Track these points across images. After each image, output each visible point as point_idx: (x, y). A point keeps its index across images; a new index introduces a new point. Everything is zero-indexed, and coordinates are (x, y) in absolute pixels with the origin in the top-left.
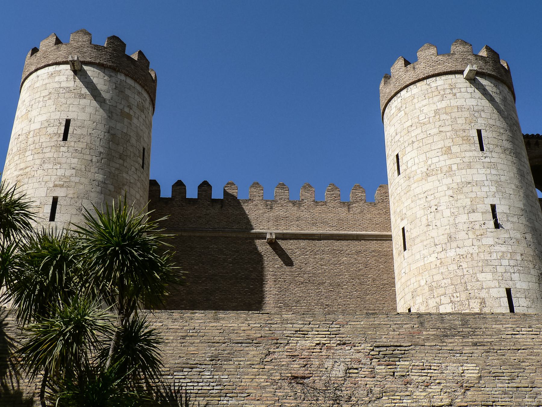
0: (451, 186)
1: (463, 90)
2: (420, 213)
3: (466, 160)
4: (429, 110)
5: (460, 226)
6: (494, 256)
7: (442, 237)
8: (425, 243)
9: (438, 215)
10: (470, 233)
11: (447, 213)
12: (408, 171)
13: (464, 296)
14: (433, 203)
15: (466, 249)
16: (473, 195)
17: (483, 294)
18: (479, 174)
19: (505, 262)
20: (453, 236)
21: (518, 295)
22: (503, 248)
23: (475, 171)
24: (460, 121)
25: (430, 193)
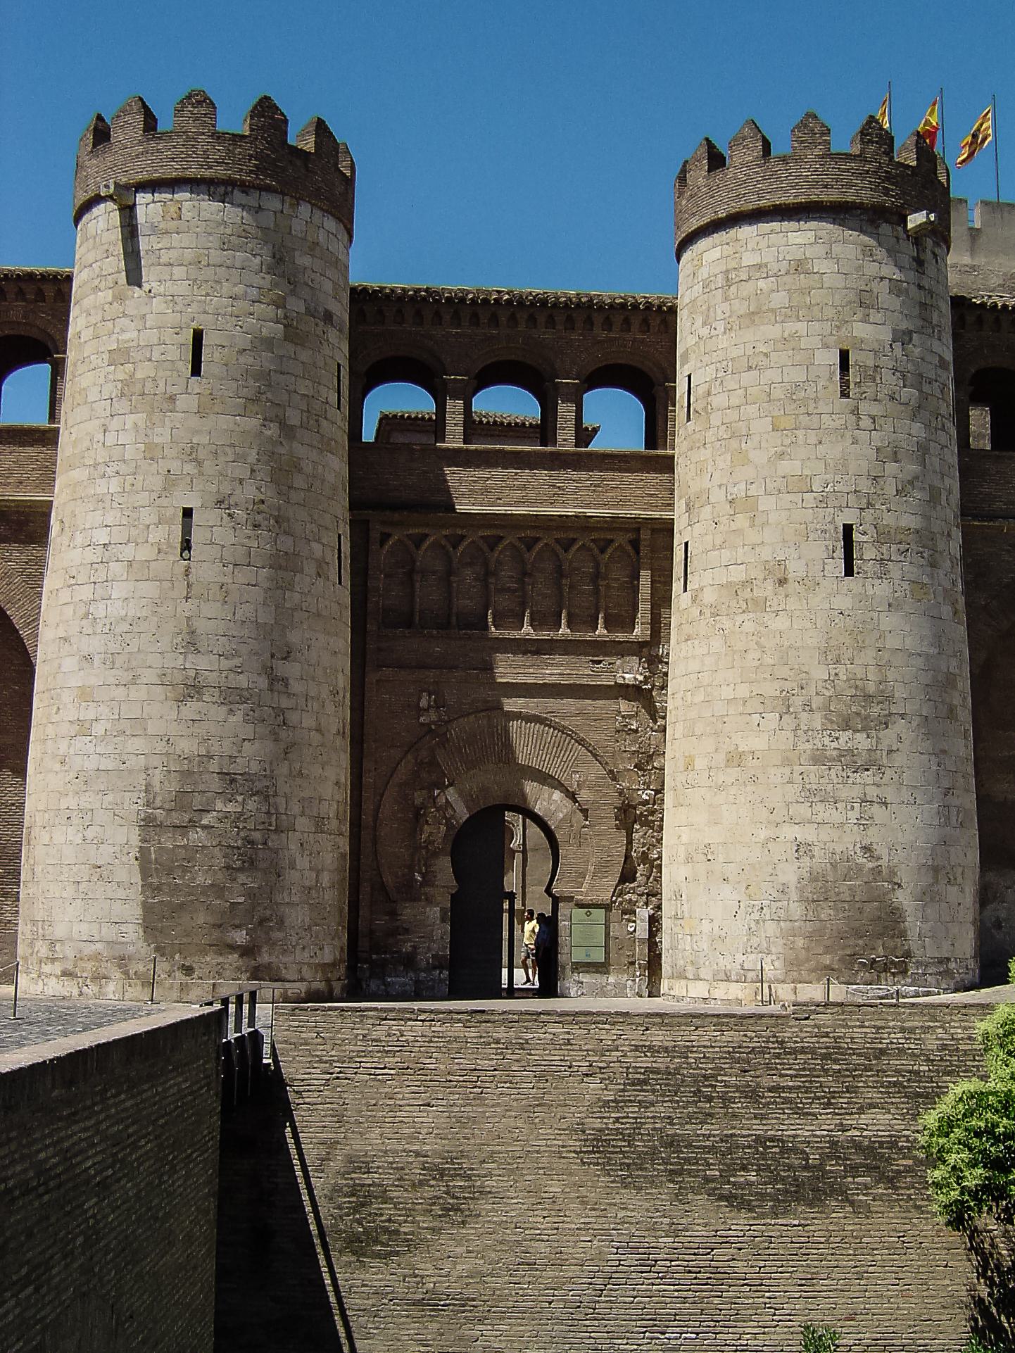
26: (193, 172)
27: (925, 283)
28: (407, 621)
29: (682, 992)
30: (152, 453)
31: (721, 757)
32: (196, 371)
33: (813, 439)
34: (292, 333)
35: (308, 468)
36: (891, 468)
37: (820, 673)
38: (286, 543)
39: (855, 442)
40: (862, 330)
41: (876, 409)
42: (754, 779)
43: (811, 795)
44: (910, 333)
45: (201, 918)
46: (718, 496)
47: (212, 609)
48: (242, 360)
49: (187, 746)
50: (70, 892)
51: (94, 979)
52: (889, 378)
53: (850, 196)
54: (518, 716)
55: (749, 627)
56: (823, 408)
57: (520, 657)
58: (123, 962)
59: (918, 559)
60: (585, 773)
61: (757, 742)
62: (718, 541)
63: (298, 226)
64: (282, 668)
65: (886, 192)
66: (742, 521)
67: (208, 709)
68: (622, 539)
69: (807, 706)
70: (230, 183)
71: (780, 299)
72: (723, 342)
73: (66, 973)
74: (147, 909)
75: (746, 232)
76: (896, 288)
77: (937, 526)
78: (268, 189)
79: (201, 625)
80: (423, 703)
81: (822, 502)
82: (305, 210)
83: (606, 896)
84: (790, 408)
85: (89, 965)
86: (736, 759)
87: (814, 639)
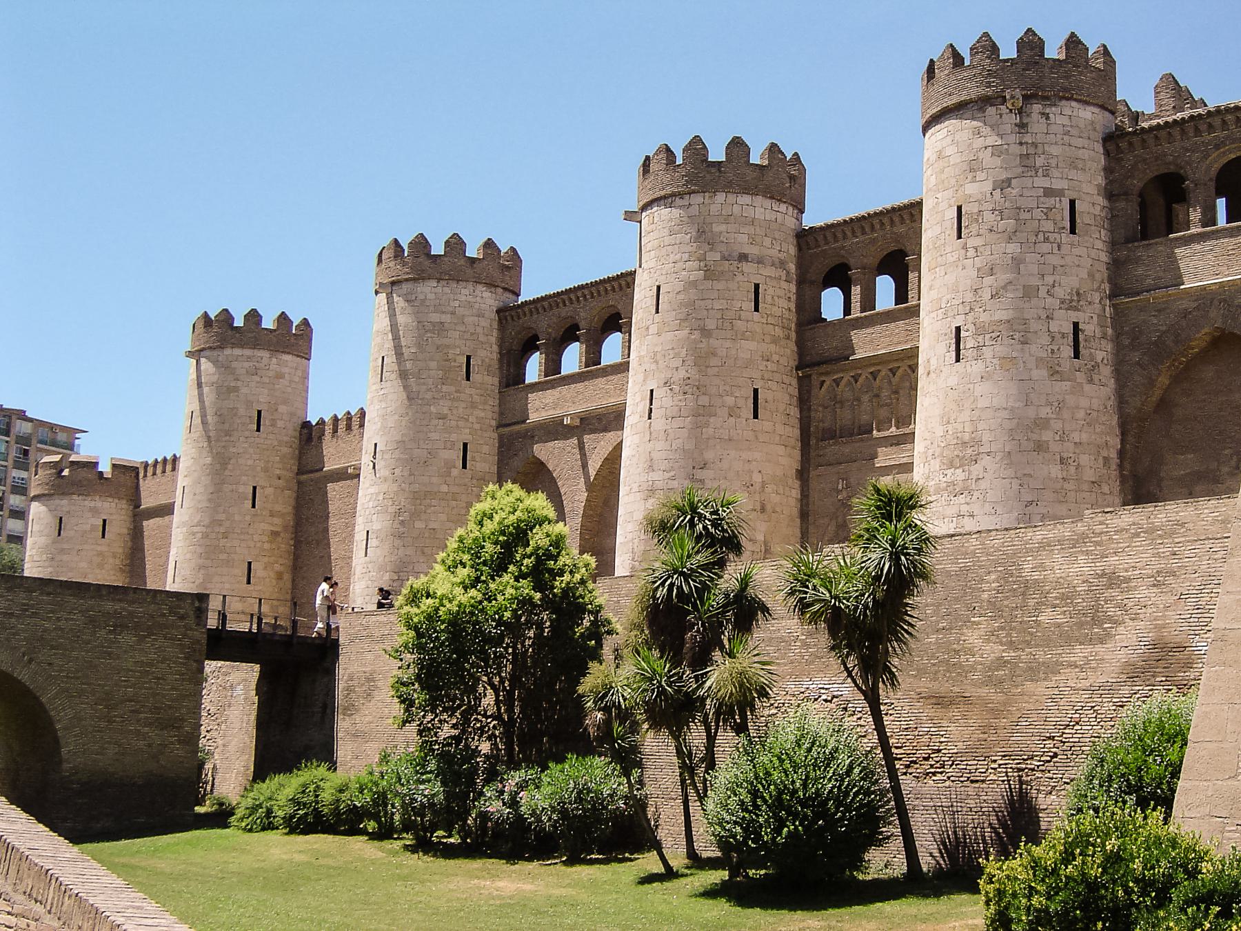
19: (371, 504)
26: (657, 195)
27: (1028, 138)
28: (831, 435)
32: (657, 312)
34: (710, 274)
35: (722, 352)
36: (988, 280)
38: (704, 400)
39: (964, 268)
40: (971, 189)
41: (978, 242)
44: (1009, 181)
47: (660, 445)
48: (679, 297)
52: (988, 216)
53: (964, 97)
56: (949, 249)
57: (889, 449)
59: (1007, 341)
63: (714, 209)
64: (700, 474)
65: (989, 85)
70: (673, 195)
76: (997, 151)
77: (1030, 314)
78: (694, 192)
79: (655, 455)
80: (840, 487)
82: (720, 197)
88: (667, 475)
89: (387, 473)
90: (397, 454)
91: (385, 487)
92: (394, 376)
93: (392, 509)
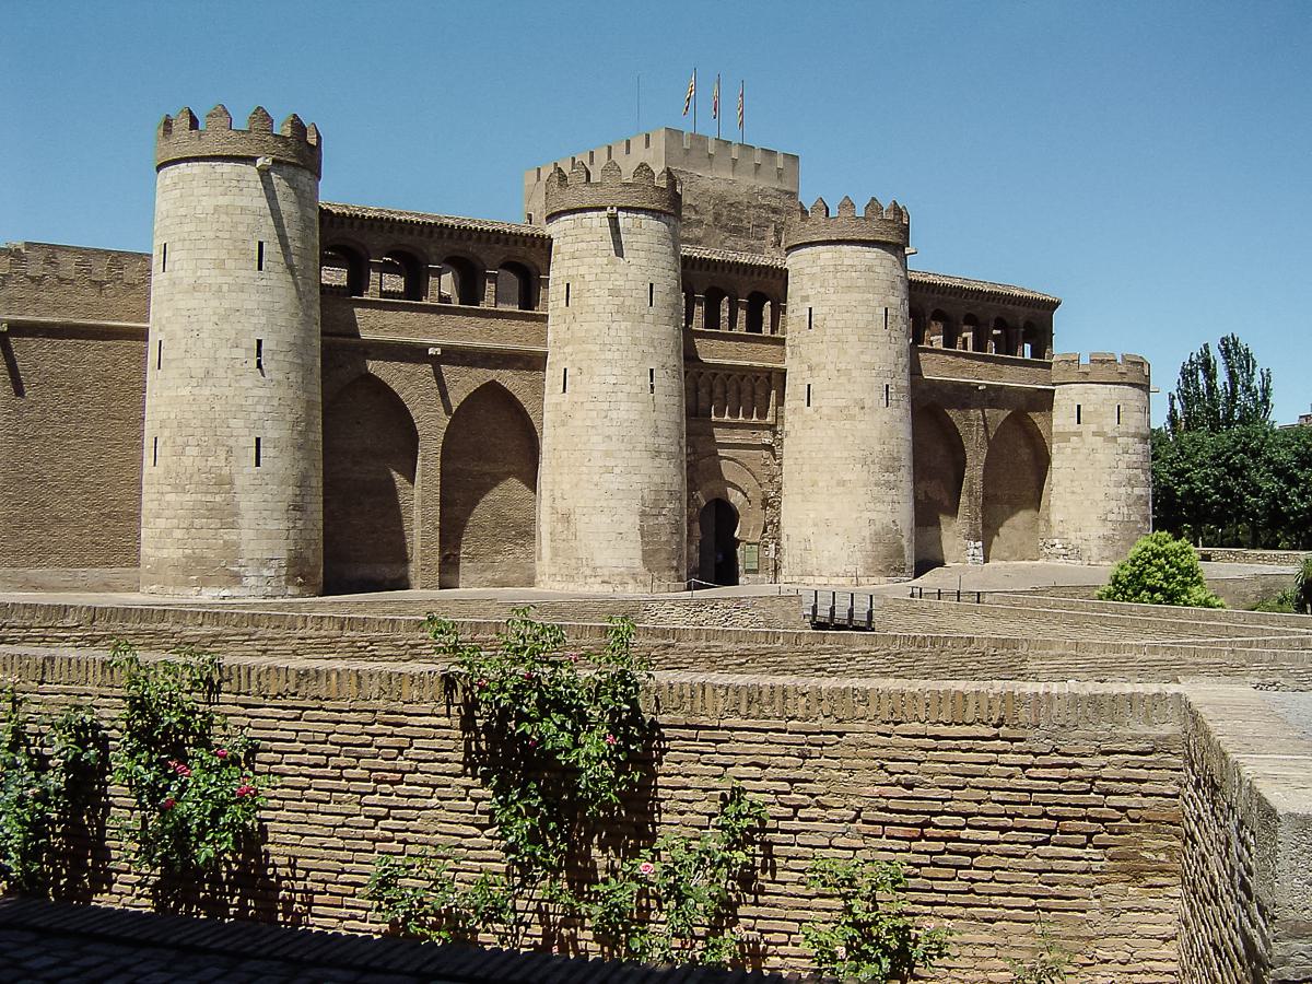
0: (218, 311)
1: (252, 184)
2: (180, 334)
3: (239, 281)
4: (208, 203)
5: (220, 362)
6: (250, 401)
7: (199, 370)
8: (182, 371)
9: (199, 343)
10: (229, 371)
11: (208, 344)
12: (174, 274)
13: (211, 442)
14: (195, 326)
15: (222, 389)
16: (239, 327)
17: (231, 442)
18: (251, 301)
19: (260, 408)
20: (211, 372)
21: (267, 445)
22: (261, 392)
23: (245, 296)
24: (241, 228)
25: (195, 313)
26: (647, 205)
29: (552, 582)
30: (635, 341)
31: (834, 482)
33: (875, 346)
37: (878, 448)
40: (892, 299)
42: (851, 492)
43: (875, 499)
45: (664, 555)
46: (830, 367)
47: (663, 416)
49: (657, 479)
50: (605, 544)
51: (621, 584)
54: (725, 458)
55: (847, 426)
58: (634, 576)
60: (747, 482)
61: (853, 477)
62: (831, 387)
66: (843, 380)
67: (662, 461)
68: (763, 377)
69: (873, 462)
70: (660, 211)
71: (861, 282)
72: (834, 297)
73: (603, 582)
74: (643, 551)
75: (846, 248)
79: (660, 424)
81: (878, 375)
83: (757, 540)
84: (866, 332)
85: (618, 578)
86: (841, 483)
87: (875, 434)
88: (668, 441)
89: (281, 377)
90: (290, 357)
91: (280, 392)
92: (280, 268)
93: (289, 417)
